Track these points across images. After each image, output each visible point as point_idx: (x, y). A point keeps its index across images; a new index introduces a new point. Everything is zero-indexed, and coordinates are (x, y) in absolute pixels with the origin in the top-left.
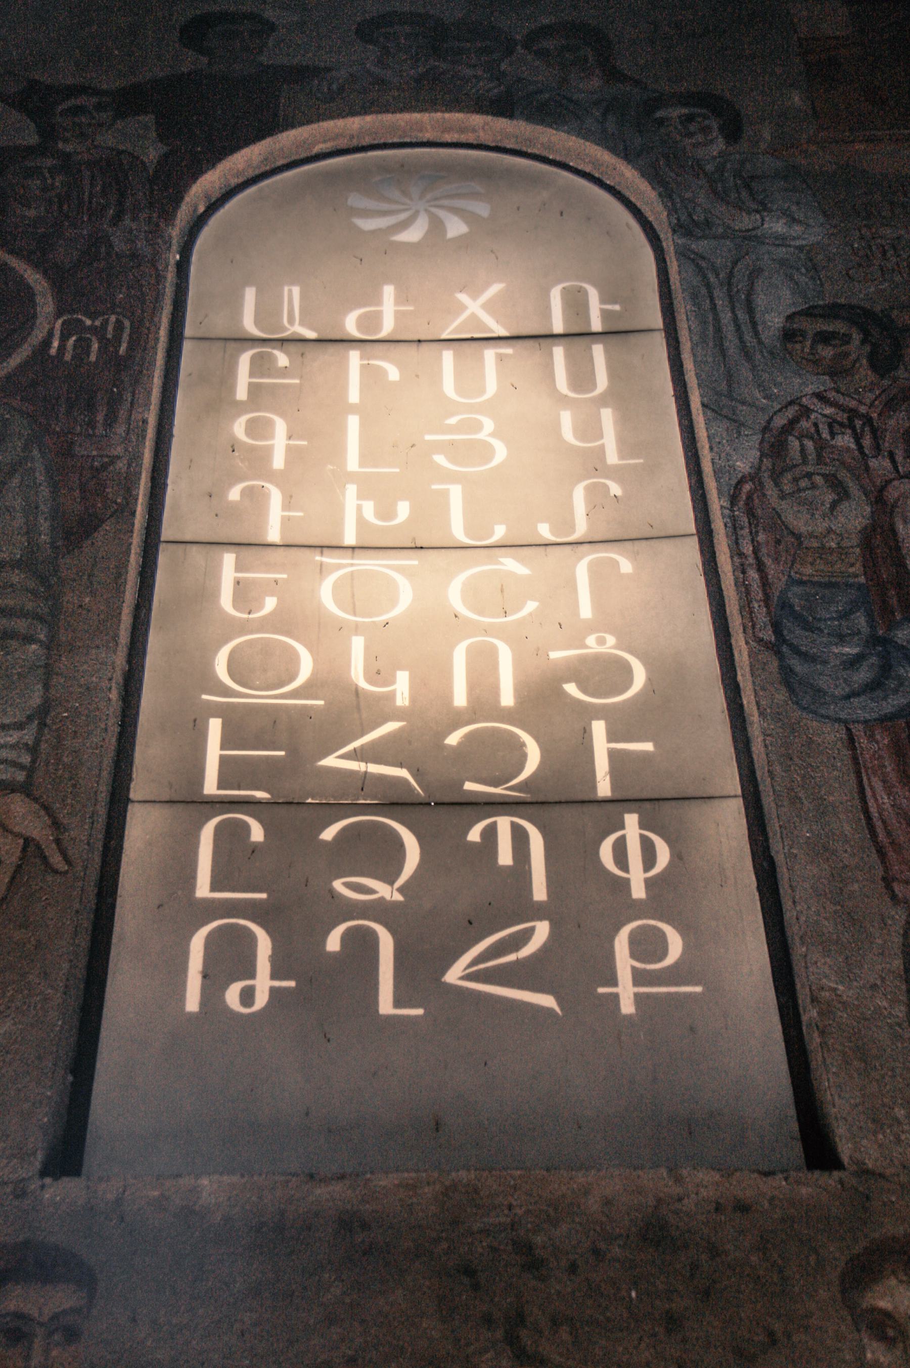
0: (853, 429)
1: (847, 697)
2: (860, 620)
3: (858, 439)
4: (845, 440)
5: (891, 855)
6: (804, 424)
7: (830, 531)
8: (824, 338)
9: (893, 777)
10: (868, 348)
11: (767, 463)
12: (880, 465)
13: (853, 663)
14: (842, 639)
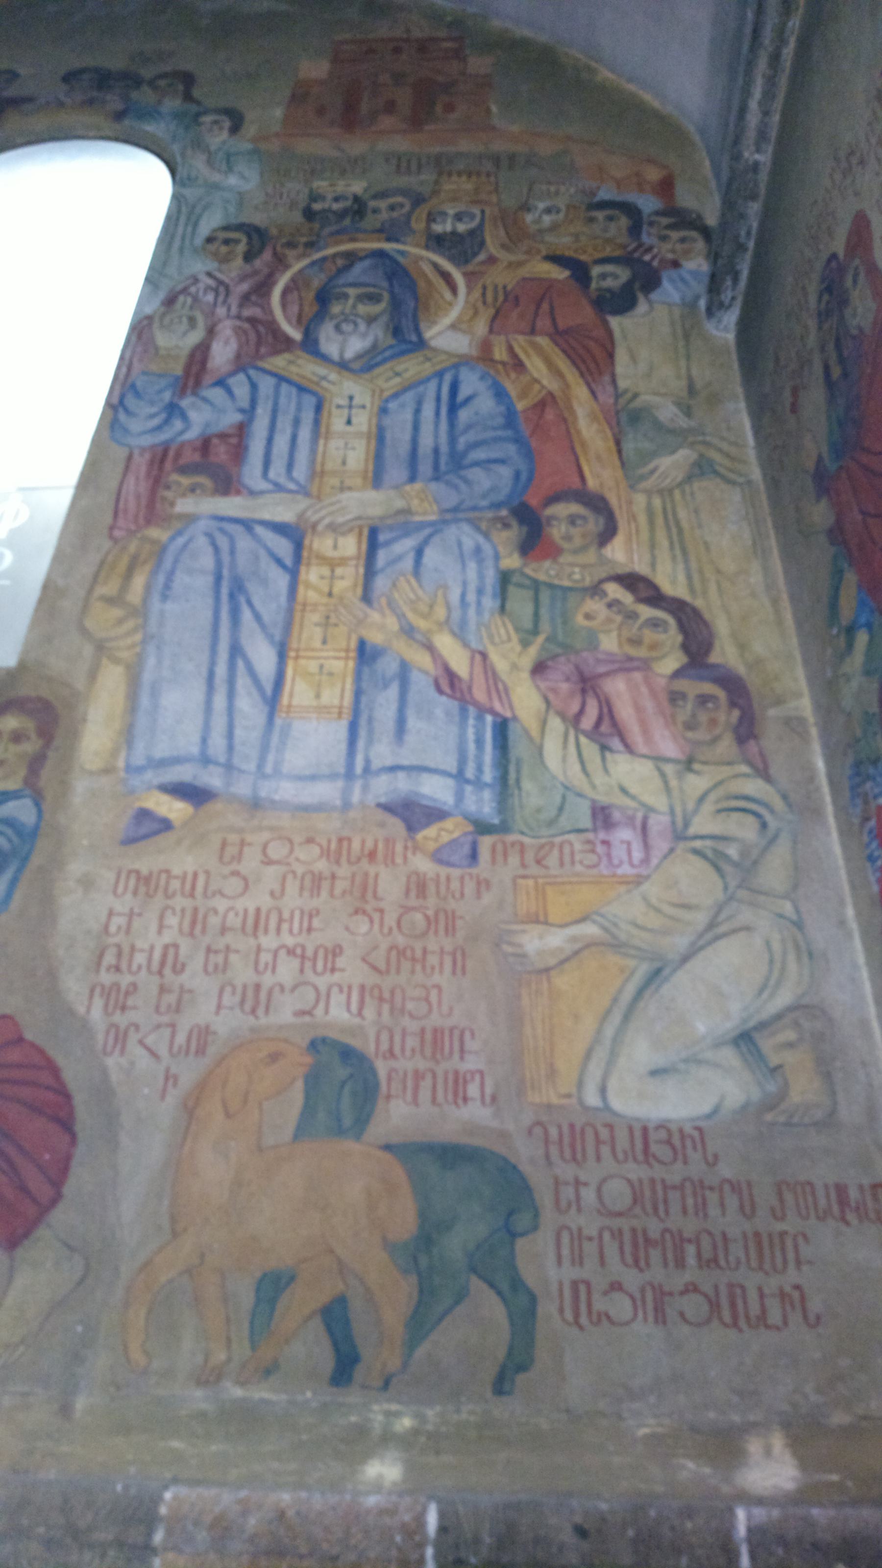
4: (210, 297)
5: (121, 515)
6: (193, 289)
8: (226, 242)
11: (163, 309)
12: (221, 311)
13: (152, 416)
14: (152, 403)
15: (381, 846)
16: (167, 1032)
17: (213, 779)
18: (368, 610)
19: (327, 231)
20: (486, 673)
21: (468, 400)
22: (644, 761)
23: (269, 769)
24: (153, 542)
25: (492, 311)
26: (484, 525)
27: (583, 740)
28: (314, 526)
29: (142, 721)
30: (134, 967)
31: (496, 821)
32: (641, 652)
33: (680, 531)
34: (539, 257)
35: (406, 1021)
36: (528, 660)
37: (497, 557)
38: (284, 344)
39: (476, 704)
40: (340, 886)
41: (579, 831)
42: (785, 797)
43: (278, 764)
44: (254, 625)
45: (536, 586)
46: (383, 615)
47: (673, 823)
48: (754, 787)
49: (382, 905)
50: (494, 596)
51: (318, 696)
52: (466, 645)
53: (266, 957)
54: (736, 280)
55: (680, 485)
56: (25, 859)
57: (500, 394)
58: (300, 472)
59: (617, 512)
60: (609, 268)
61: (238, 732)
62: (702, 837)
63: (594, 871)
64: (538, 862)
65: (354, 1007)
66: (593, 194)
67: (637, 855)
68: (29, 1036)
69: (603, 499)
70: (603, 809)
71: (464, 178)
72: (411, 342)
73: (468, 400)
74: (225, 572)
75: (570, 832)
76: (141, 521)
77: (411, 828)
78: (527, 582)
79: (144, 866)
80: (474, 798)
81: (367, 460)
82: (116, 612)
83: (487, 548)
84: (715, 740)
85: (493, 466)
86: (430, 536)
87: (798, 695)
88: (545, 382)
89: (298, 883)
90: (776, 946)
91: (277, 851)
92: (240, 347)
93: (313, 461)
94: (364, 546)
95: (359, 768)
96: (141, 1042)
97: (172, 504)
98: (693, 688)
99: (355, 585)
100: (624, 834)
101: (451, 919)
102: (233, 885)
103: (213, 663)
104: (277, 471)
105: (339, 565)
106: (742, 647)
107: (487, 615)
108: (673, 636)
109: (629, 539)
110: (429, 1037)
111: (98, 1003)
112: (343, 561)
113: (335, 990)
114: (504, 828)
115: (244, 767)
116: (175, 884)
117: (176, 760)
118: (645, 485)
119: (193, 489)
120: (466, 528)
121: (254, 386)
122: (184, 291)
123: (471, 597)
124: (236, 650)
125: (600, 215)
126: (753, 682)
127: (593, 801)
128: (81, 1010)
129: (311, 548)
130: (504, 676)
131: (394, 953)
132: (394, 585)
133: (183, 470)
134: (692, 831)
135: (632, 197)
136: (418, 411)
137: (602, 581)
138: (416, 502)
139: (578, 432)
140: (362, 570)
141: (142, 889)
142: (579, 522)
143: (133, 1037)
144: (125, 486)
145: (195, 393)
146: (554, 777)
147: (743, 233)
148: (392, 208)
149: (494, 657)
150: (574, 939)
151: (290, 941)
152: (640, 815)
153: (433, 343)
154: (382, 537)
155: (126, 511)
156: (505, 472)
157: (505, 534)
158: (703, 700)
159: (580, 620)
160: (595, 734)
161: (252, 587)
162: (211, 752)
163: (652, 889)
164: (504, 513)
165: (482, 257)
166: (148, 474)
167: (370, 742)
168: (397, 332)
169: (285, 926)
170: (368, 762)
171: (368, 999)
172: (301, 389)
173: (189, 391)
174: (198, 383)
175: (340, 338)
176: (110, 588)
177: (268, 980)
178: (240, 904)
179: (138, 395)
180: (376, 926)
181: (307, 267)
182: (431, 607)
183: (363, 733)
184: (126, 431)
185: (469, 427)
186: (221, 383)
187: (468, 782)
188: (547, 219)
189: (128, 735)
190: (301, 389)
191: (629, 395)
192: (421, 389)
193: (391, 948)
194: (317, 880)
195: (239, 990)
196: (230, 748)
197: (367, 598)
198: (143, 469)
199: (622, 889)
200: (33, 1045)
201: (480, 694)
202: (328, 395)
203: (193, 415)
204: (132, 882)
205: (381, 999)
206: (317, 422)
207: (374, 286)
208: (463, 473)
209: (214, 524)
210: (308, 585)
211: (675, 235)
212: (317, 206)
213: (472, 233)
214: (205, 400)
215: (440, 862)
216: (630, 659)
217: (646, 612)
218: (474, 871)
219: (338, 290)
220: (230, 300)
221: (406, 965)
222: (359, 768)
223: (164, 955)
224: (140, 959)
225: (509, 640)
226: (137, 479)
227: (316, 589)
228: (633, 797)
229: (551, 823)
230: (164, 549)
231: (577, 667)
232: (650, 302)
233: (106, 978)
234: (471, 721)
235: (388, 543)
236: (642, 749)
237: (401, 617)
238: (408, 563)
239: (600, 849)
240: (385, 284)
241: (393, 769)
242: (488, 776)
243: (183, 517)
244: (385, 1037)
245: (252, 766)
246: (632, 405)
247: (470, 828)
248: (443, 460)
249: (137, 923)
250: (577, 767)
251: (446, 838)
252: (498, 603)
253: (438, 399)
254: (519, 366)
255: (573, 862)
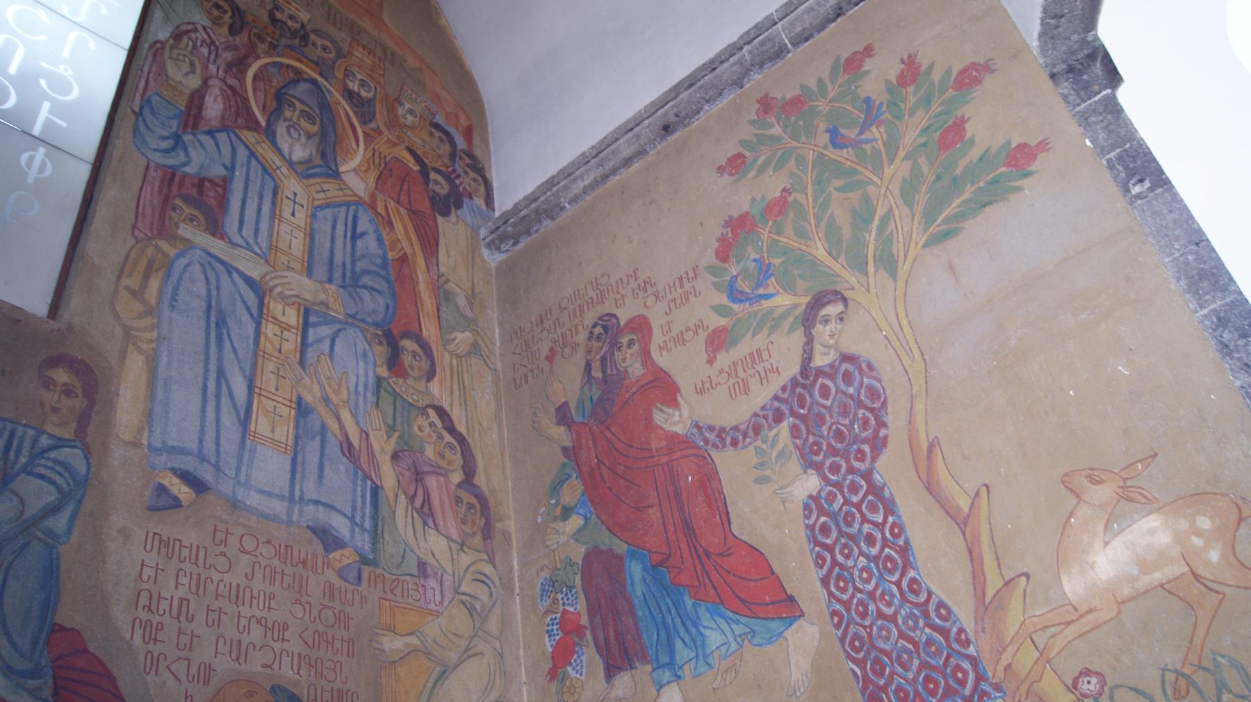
0: (210, 48)
1: (155, 150)
2: (174, 123)
3: (210, 53)
4: (205, 51)
5: (140, 218)
6: (193, 35)
7: (181, 82)
9: (156, 188)
10: (231, 21)
15: (309, 557)
16: (186, 662)
17: (207, 475)
18: (304, 376)
19: (284, 41)
20: (368, 449)
21: (363, 234)
22: (443, 538)
23: (243, 479)
24: (165, 255)
25: (376, 173)
26: (369, 336)
27: (415, 514)
28: (271, 291)
29: (158, 410)
30: (161, 611)
31: (371, 557)
32: (443, 463)
33: (464, 388)
34: (404, 146)
35: (323, 682)
36: (390, 449)
37: (375, 365)
38: (253, 125)
39: (363, 470)
40: (287, 580)
41: (411, 575)
42: (500, 579)
43: (248, 476)
44: (232, 356)
45: (395, 395)
46: (312, 380)
47: (454, 582)
48: (488, 569)
49: (310, 600)
50: (373, 393)
51: (273, 431)
52: (357, 423)
53: (244, 622)
54: (515, 244)
55: (465, 356)
56: (80, 502)
57: (380, 240)
58: (263, 239)
59: (436, 362)
60: (439, 178)
61: (222, 442)
62: (466, 594)
63: (418, 604)
64: (391, 591)
65: (295, 667)
66: (434, 115)
67: (438, 598)
68: (91, 649)
69: (430, 348)
70: (423, 564)
71: (366, 53)
72: (331, 169)
73: (363, 234)
74: (214, 304)
75: (407, 575)
76: (155, 232)
77: (327, 549)
78: (390, 390)
79: (166, 531)
80: (360, 538)
81: (304, 251)
82: (137, 307)
83: (369, 353)
84: (474, 534)
85: (375, 293)
86: (339, 330)
87: (509, 518)
88: (405, 244)
89: (262, 570)
90: (492, 669)
91: (249, 544)
92: (225, 109)
93: (271, 235)
94: (301, 322)
95: (297, 498)
96: (168, 667)
97: (177, 227)
98: (462, 493)
99: (295, 351)
100: (432, 583)
101: (348, 618)
102: (222, 563)
103: (206, 379)
104: (248, 231)
105: (286, 329)
106: (488, 479)
107: (369, 407)
108: (458, 459)
109: (441, 383)
110: (335, 694)
111: (138, 633)
112: (287, 328)
113: (284, 653)
114: (374, 563)
115: (227, 471)
116: (185, 552)
117: (183, 451)
118: (451, 347)
119: (192, 219)
120: (359, 334)
121: (234, 149)
122: (188, 32)
123: (361, 389)
124: (221, 373)
125: (437, 134)
126: (491, 501)
127: (419, 557)
128: (128, 636)
129: (269, 308)
130: (377, 455)
131: (317, 634)
132: (318, 361)
133: (187, 199)
134: (462, 589)
135: (452, 130)
136: (334, 227)
137: (427, 406)
138: (332, 300)
139: (420, 293)
140: (299, 340)
141: (164, 551)
142: (417, 358)
143: (163, 665)
144: (143, 194)
145: (194, 135)
146: (400, 536)
147: (535, 228)
148: (325, 49)
149: (372, 438)
150: (407, 645)
151: (258, 614)
152: (439, 572)
153: (344, 177)
154: (312, 319)
155: (144, 215)
156: (381, 301)
157: (380, 348)
158: (471, 506)
159: (416, 428)
160: (420, 511)
161: (232, 325)
162: (205, 452)
163: (442, 620)
164: (380, 333)
165: (373, 125)
166: (160, 192)
167: (303, 477)
168: (323, 155)
169: (255, 601)
170: (302, 492)
171: (302, 663)
172: (265, 170)
173: (189, 130)
174: (195, 127)
175: (290, 140)
176: (132, 281)
177: (245, 639)
178: (226, 577)
179: (153, 113)
180: (307, 615)
181: (269, 64)
182: (339, 386)
183: (299, 469)
184: (144, 141)
185: (363, 257)
186: (209, 133)
187: (356, 524)
188: (410, 118)
189: (149, 417)
190: (265, 170)
191: (444, 279)
192: (336, 209)
193: (315, 631)
194: (274, 572)
195: (228, 641)
196: (218, 453)
197: (302, 363)
198: (157, 184)
199: (430, 618)
200: (93, 654)
201: (365, 466)
202: (281, 185)
203: (192, 152)
204: (156, 542)
205: (310, 665)
206: (274, 203)
207: (311, 109)
208: (358, 289)
209: (205, 256)
210: (267, 339)
211: (472, 174)
212: (278, 15)
213: (370, 100)
214: (199, 142)
215: (341, 577)
216: (440, 467)
217: (448, 438)
218: (360, 589)
219: (287, 97)
220: (218, 62)
221: (323, 645)
222: (297, 498)
223: (180, 606)
224: (164, 605)
225: (380, 430)
226: (152, 189)
227: (271, 343)
228: (437, 561)
229: (399, 566)
230: (172, 264)
231: (414, 462)
232: (457, 217)
233: (144, 615)
234: (359, 482)
235: (316, 325)
236: (442, 529)
237: (322, 387)
238: (326, 346)
239: (421, 590)
240: (317, 111)
241: (317, 502)
242: (367, 525)
243: (184, 240)
244: (312, 691)
245: (232, 473)
246: (446, 287)
247: (358, 559)
248: (348, 274)
249: (161, 575)
250: (412, 532)
251: (345, 562)
252: (375, 400)
253: (346, 225)
254: (390, 224)
255: (408, 597)
